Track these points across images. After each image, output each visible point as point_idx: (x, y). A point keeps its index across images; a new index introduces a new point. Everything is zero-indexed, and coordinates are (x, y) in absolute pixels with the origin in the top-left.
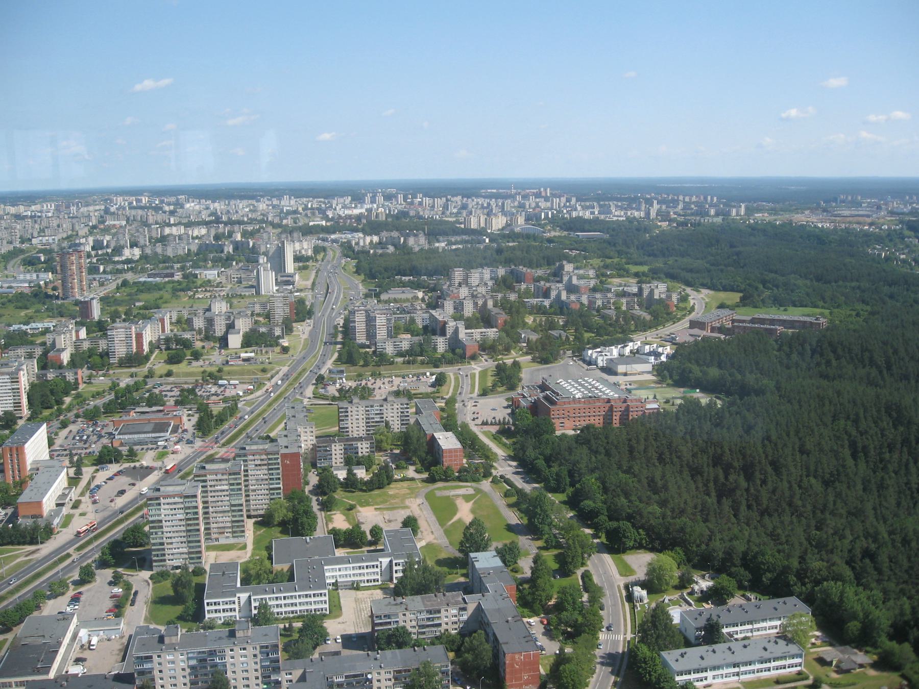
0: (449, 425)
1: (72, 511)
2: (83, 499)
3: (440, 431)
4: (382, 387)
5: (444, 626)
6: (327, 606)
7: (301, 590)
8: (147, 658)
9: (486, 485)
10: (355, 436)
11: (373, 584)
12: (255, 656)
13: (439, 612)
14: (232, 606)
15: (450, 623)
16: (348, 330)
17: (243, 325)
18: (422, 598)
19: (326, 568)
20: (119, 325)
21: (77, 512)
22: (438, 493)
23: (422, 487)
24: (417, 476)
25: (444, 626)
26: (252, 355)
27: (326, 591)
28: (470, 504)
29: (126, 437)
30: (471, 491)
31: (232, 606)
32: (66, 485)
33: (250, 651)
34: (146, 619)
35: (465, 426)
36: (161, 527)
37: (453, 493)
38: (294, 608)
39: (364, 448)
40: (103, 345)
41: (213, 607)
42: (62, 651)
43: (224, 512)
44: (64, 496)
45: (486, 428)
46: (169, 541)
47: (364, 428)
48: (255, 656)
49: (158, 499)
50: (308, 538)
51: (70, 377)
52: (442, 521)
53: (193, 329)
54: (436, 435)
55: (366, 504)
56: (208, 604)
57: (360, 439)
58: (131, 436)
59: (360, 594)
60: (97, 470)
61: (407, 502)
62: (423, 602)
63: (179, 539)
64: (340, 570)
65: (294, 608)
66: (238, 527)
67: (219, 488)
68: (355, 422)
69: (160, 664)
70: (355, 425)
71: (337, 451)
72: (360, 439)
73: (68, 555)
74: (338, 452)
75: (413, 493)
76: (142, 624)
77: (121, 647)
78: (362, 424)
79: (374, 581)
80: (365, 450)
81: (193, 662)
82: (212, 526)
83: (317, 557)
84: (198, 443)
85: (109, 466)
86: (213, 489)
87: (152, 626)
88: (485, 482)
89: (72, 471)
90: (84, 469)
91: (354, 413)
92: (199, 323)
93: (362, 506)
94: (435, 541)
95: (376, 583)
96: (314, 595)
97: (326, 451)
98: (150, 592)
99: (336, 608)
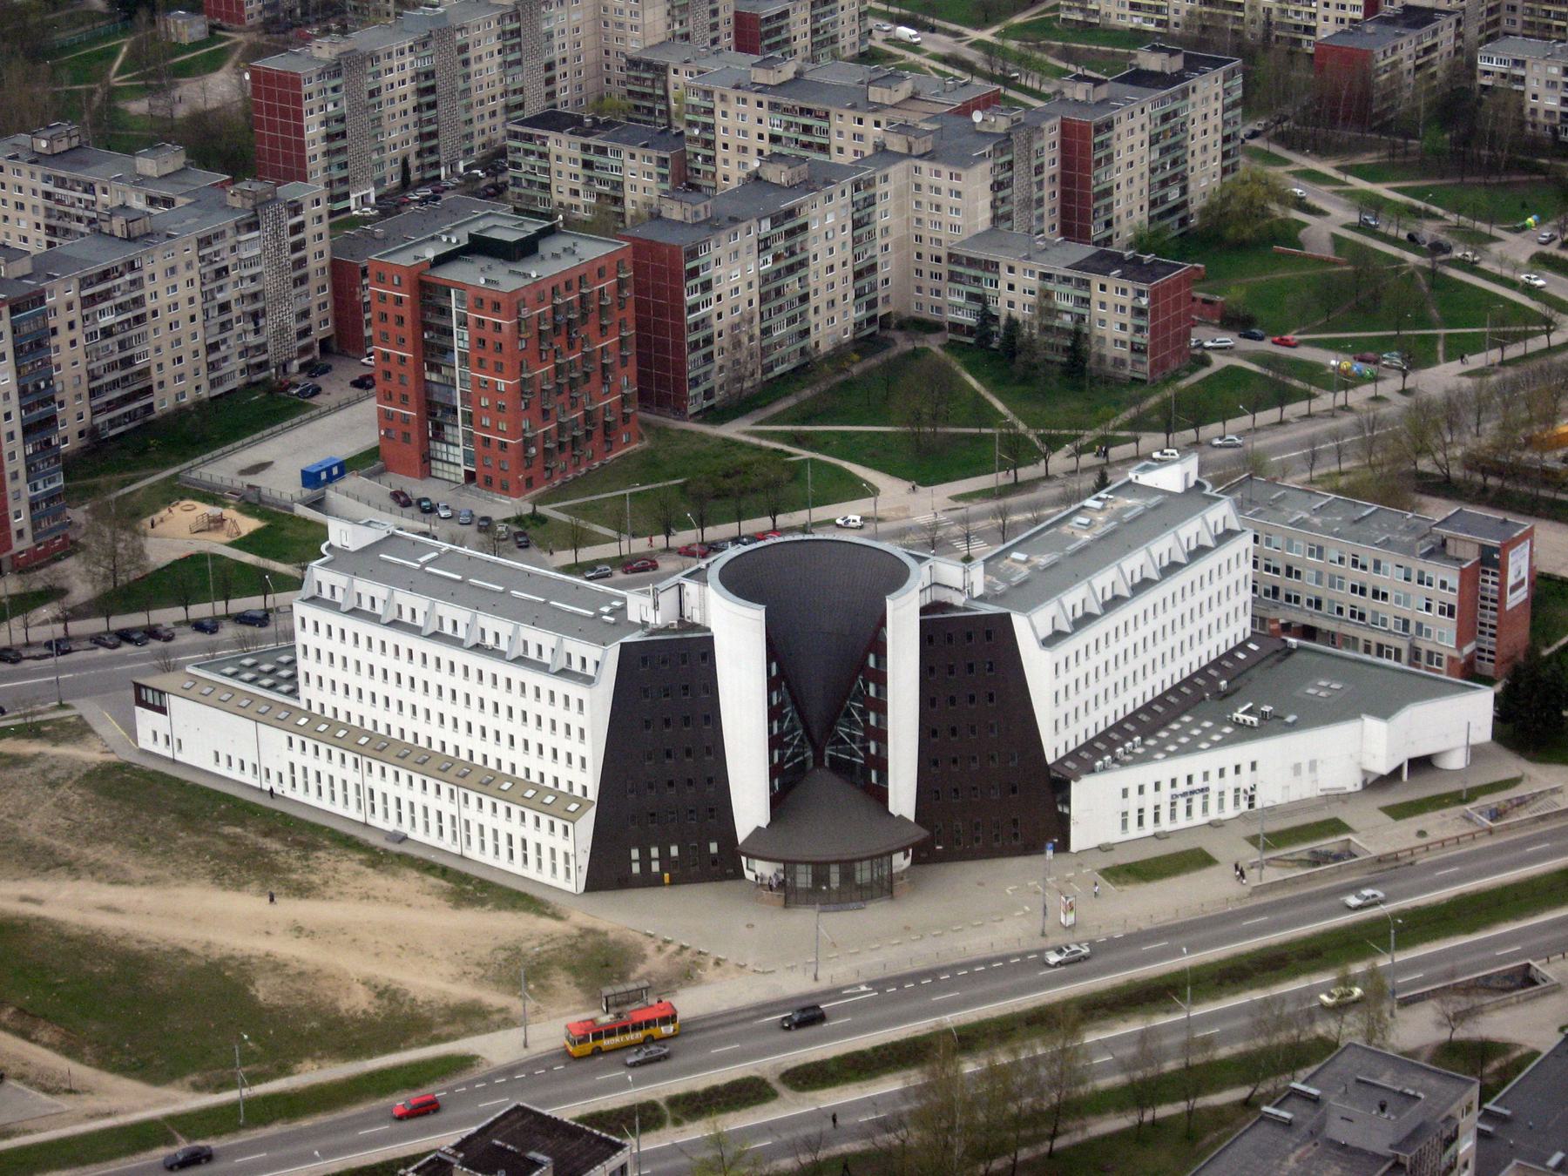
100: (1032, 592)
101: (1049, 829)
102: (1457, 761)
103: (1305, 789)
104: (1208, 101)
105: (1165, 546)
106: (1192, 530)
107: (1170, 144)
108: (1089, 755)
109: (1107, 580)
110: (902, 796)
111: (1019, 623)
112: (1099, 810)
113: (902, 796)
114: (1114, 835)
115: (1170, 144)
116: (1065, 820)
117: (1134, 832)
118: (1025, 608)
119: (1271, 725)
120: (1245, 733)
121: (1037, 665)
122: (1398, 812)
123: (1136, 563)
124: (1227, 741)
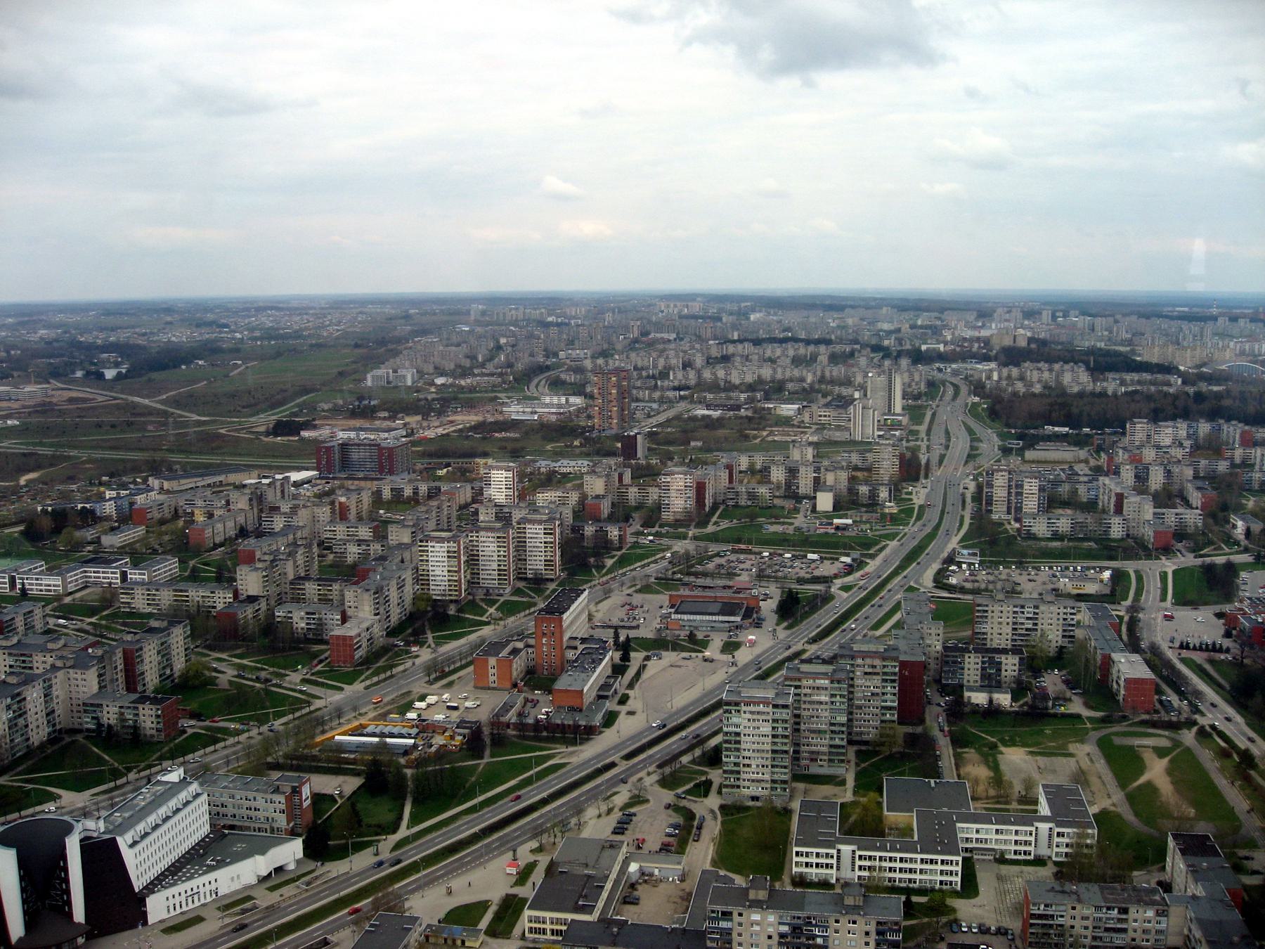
0: (1133, 645)
1: (618, 708)
2: (631, 693)
3: (1122, 651)
4: (1033, 580)
5: (1131, 934)
6: (959, 879)
7: (922, 852)
8: (724, 913)
9: (1188, 737)
10: (995, 646)
11: (1022, 857)
12: (867, 934)
13: (1125, 911)
14: (829, 861)
15: (1139, 931)
16: (982, 497)
17: (837, 479)
18: (1102, 889)
19: (959, 825)
20: (676, 469)
21: (624, 709)
22: (1118, 741)
23: (1094, 729)
24: (1086, 713)
25: (1131, 934)
26: (849, 521)
27: (960, 859)
28: (1165, 761)
29: (685, 617)
30: (1164, 743)
31: (829, 861)
32: (609, 672)
33: (861, 926)
34: (714, 863)
35: (1154, 649)
36: (739, 742)
37: (1137, 742)
38: (912, 876)
39: (1010, 665)
40: (653, 494)
41: (804, 860)
42: (609, 886)
43: (820, 732)
44: (605, 686)
45: (1185, 653)
46: (747, 761)
47: (1009, 637)
48: (867, 934)
49: (737, 704)
50: (932, 781)
51: (614, 532)
52: (1123, 783)
53: (769, 482)
54: (1115, 656)
55: (1012, 743)
56: (797, 853)
57: (1004, 651)
58: (692, 617)
59: (1005, 869)
60: (647, 658)
61: (1072, 748)
62: (1102, 893)
63: (760, 761)
64: (977, 831)
65: (912, 876)
66: (838, 754)
67: (815, 698)
68: (996, 626)
69: (740, 924)
70: (996, 630)
71: (972, 665)
72: (1004, 651)
73: (612, 765)
74: (972, 666)
75: (1081, 738)
76: (708, 867)
77: (681, 893)
78: (1008, 630)
79: (1025, 853)
80: (1010, 668)
81: (785, 929)
82: (803, 748)
83: (945, 809)
84: (782, 634)
85: (664, 653)
86: (808, 699)
87: (722, 873)
88: (1185, 731)
89: (617, 655)
90: (632, 654)
91: (997, 614)
92: (778, 475)
93: (1006, 745)
94: (1112, 808)
95: (1028, 858)
96: (943, 862)
97: (955, 662)
98: (719, 827)
99: (969, 886)
100: (123, 828)
101: (141, 917)
102: (292, 867)
103: (236, 886)
104: (178, 637)
105: (173, 803)
106: (183, 795)
107: (165, 652)
108: (151, 887)
109: (152, 819)
110: (79, 915)
111: (119, 840)
112: (158, 907)
113: (79, 915)
114: (165, 916)
115: (165, 652)
116: (145, 913)
117: (173, 913)
118: (121, 835)
119: (221, 864)
120: (211, 869)
121: (128, 856)
122: (272, 889)
123: (163, 811)
124: (205, 873)
